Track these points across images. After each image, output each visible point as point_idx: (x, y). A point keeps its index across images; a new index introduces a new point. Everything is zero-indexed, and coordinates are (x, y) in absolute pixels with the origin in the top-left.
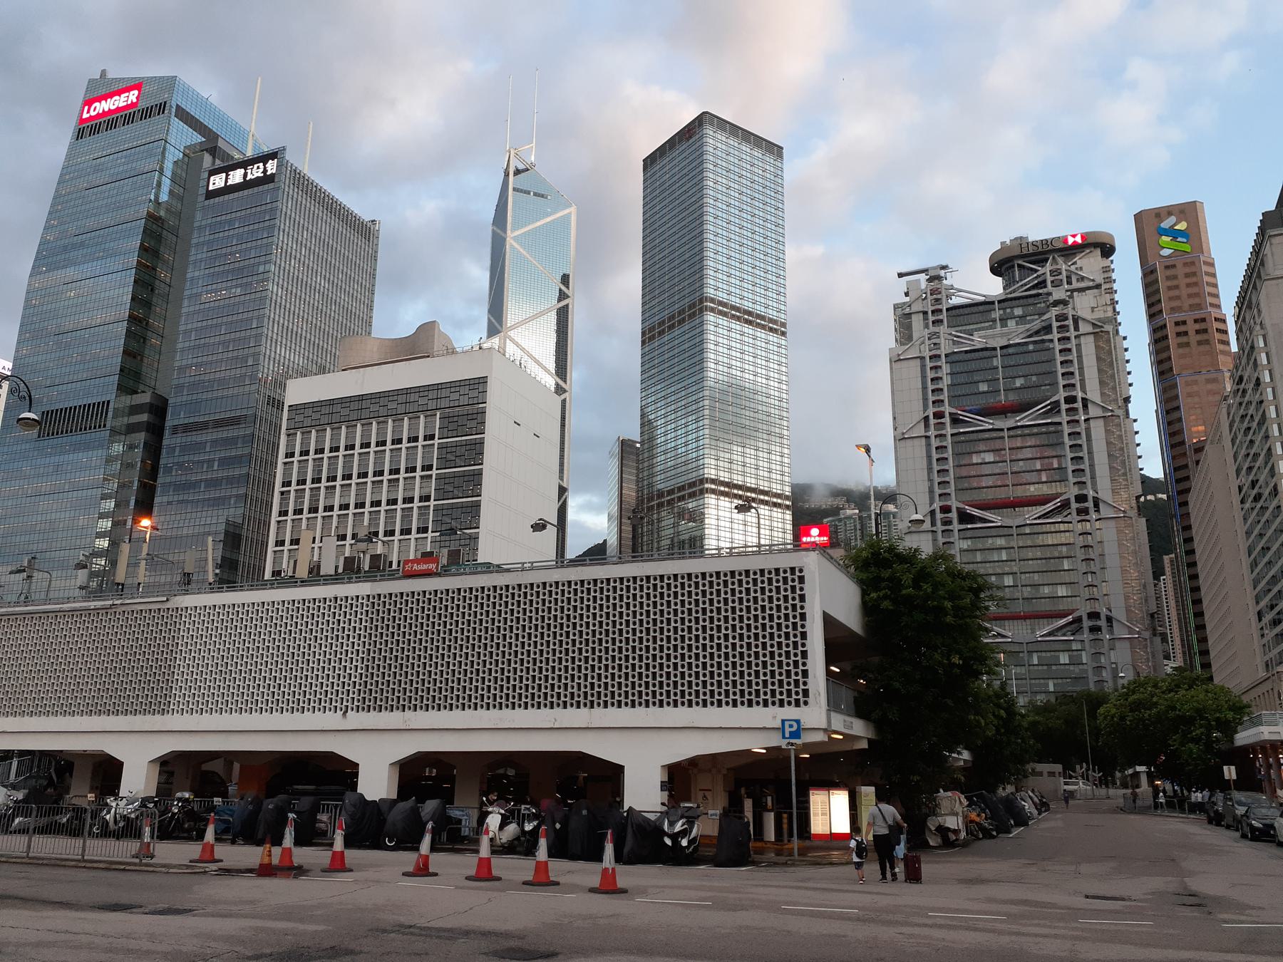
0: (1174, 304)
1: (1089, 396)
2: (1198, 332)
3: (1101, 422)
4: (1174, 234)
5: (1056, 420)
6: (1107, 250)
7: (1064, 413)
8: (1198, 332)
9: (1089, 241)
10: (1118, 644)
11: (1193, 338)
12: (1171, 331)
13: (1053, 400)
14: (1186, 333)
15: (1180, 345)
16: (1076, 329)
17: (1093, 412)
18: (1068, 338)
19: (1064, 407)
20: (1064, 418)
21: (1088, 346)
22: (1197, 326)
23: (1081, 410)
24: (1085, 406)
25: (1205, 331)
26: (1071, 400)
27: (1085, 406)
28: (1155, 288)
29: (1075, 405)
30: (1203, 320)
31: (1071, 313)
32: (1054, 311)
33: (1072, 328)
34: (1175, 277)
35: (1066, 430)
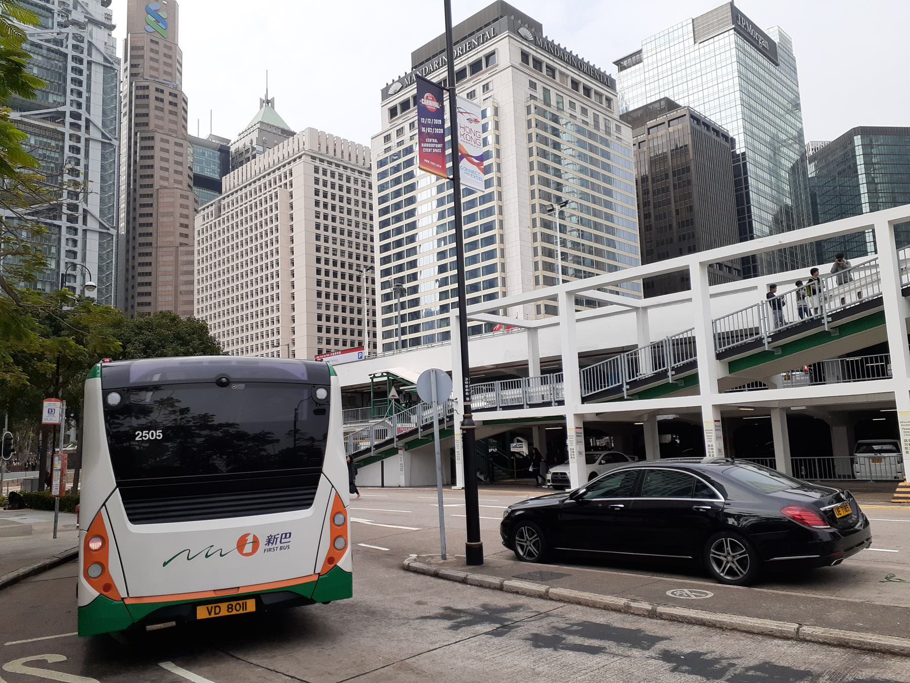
1: (92, 118)
2: (171, 103)
4: (159, 19)
5: (60, 129)
7: (67, 125)
8: (171, 103)
12: (152, 94)
13: (61, 109)
14: (162, 100)
15: (157, 108)
16: (90, 54)
17: (95, 134)
18: (81, 61)
19: (68, 120)
20: (67, 130)
21: (98, 74)
22: (171, 99)
23: (83, 128)
24: (87, 128)
25: (176, 105)
26: (76, 116)
27: (87, 128)
29: (79, 122)
30: (175, 96)
32: (71, 30)
33: (85, 51)
34: (157, 52)
35: (68, 143)
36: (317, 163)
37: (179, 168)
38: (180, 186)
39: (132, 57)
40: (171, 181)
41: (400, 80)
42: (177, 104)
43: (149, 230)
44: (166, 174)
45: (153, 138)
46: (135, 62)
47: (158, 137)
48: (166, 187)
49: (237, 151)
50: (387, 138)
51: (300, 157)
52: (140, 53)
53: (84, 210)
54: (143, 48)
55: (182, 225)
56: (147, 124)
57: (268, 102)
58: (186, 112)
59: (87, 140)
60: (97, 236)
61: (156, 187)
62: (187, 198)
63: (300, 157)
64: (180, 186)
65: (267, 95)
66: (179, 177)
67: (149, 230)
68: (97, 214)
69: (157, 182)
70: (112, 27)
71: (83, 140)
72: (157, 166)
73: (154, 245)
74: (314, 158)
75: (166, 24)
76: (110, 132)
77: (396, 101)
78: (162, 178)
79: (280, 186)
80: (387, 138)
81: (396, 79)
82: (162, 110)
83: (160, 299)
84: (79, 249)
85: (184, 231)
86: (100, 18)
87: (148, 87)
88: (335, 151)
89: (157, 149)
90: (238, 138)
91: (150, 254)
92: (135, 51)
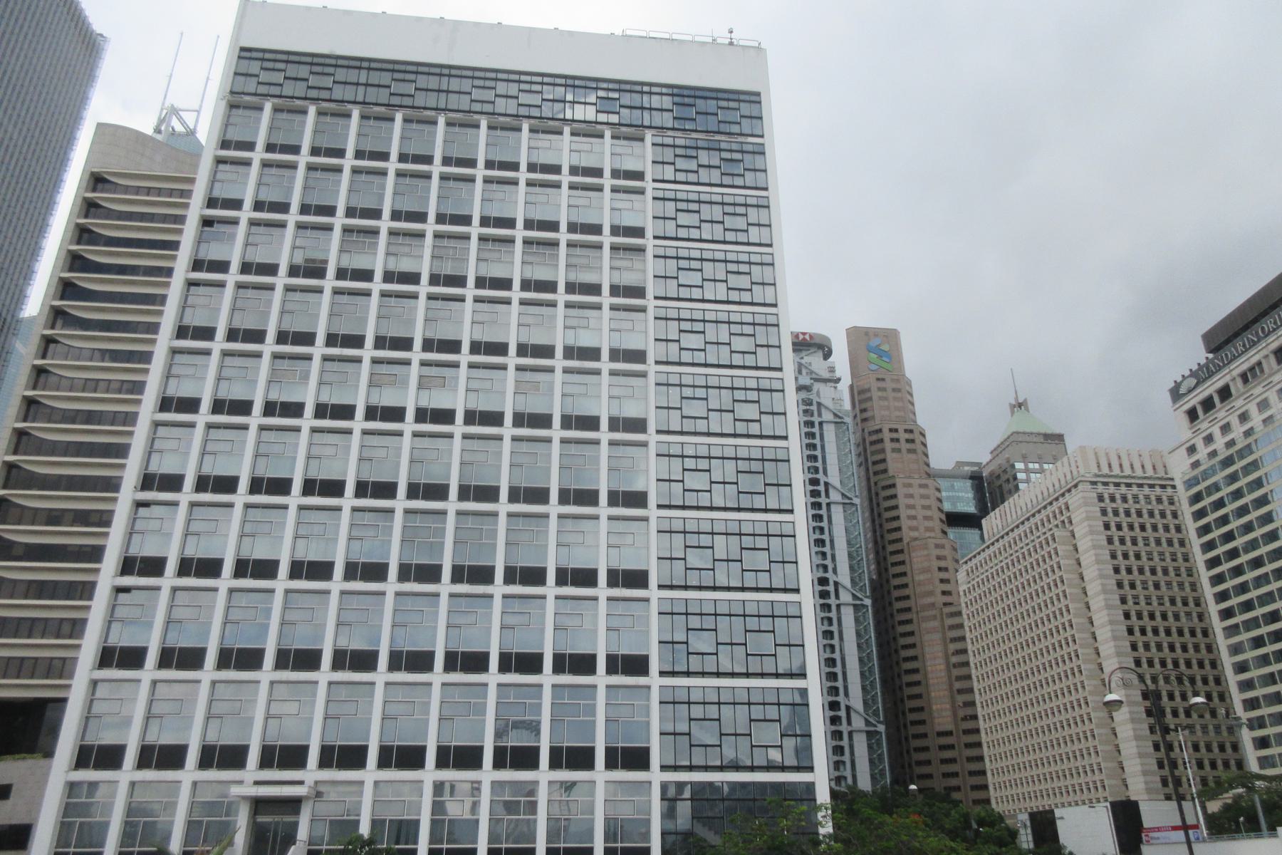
0: (886, 413)
2: (908, 441)
3: (840, 508)
4: (881, 354)
6: (828, 354)
8: (908, 441)
9: (817, 341)
10: (855, 736)
11: (904, 446)
12: (887, 436)
14: (898, 440)
15: (894, 450)
17: (835, 496)
21: (830, 432)
22: (907, 436)
23: (823, 494)
25: (913, 441)
28: (868, 395)
30: (911, 431)
31: (815, 399)
33: (816, 413)
34: (884, 390)
36: (1100, 488)
37: (929, 513)
38: (932, 534)
39: (860, 402)
40: (922, 529)
41: (1193, 374)
42: (914, 440)
43: (906, 592)
44: (914, 523)
45: (893, 486)
46: (864, 406)
47: (899, 482)
48: (916, 539)
49: (991, 474)
50: (1192, 450)
51: (1076, 486)
52: (868, 395)
53: (836, 584)
54: (869, 390)
55: (942, 581)
56: (885, 471)
57: (1020, 405)
58: (925, 445)
59: (828, 505)
60: (851, 608)
61: (905, 541)
62: (943, 547)
63: (1076, 486)
64: (932, 534)
65: (1017, 398)
66: (929, 524)
67: (906, 592)
68: (848, 585)
69: (907, 534)
70: (839, 379)
71: (824, 506)
72: (903, 516)
73: (914, 610)
74: (1094, 483)
75: (890, 358)
76: (849, 490)
77: (1194, 400)
78: (911, 529)
79: (1057, 526)
80: (1192, 450)
81: (1187, 373)
82: (899, 451)
83: (930, 676)
84: (834, 628)
85: (946, 587)
86: (826, 375)
87: (880, 431)
88: (1121, 466)
89: (900, 496)
90: (989, 457)
91: (909, 622)
92: (860, 396)
